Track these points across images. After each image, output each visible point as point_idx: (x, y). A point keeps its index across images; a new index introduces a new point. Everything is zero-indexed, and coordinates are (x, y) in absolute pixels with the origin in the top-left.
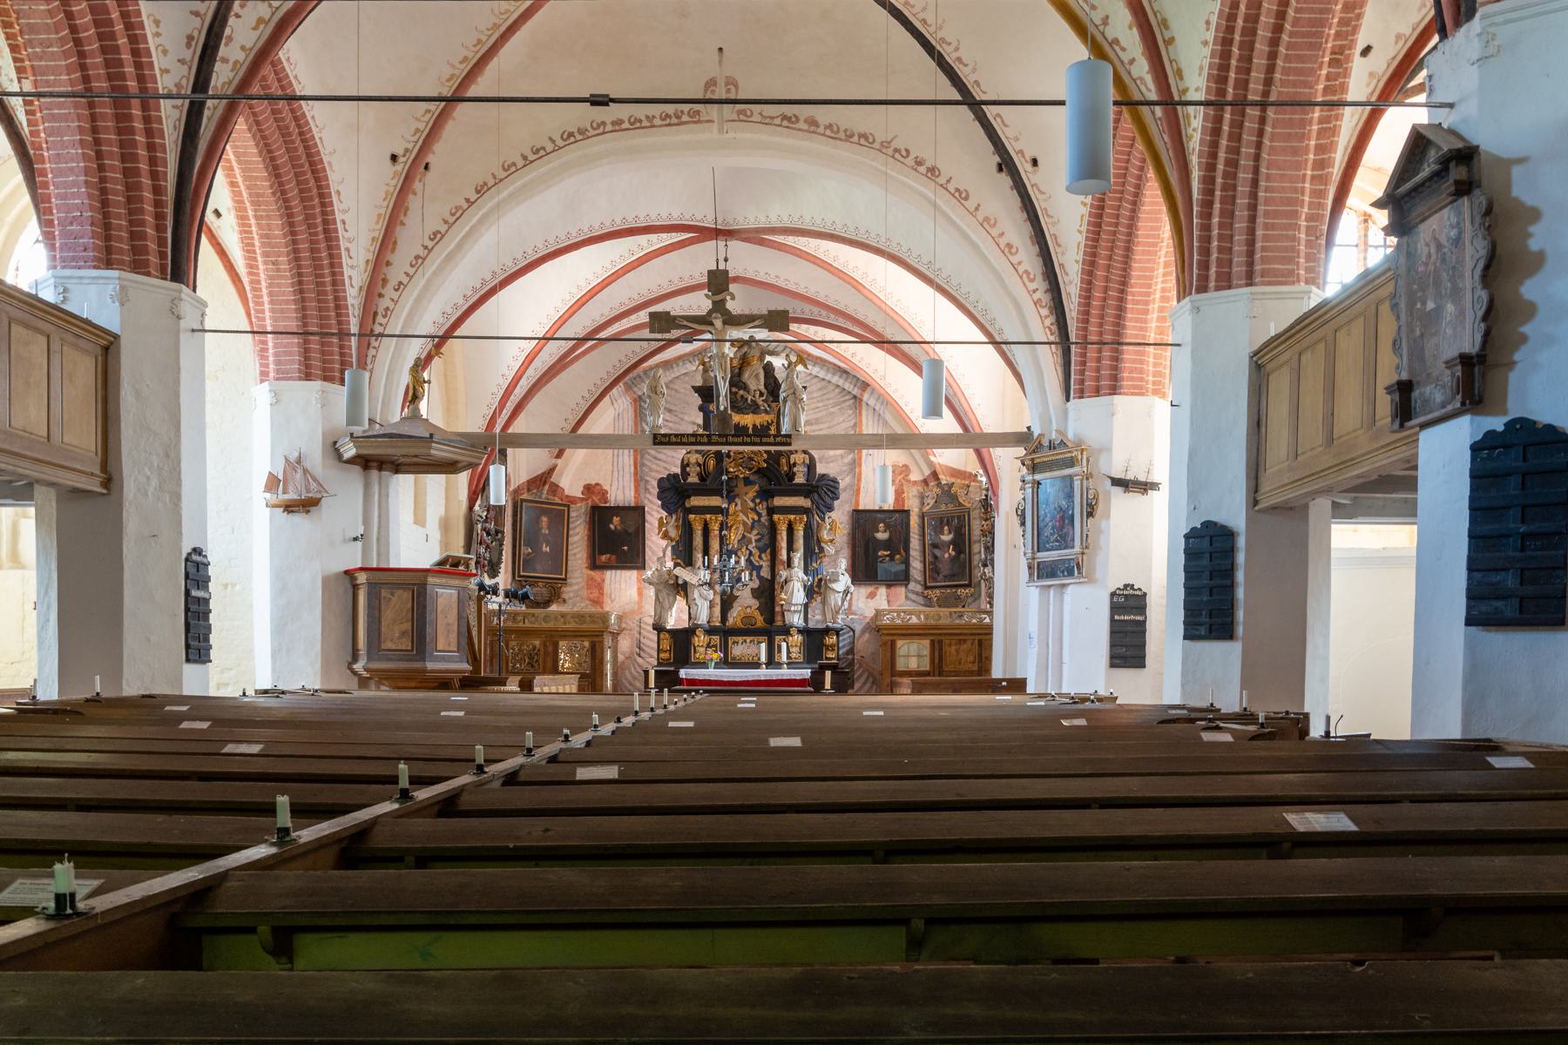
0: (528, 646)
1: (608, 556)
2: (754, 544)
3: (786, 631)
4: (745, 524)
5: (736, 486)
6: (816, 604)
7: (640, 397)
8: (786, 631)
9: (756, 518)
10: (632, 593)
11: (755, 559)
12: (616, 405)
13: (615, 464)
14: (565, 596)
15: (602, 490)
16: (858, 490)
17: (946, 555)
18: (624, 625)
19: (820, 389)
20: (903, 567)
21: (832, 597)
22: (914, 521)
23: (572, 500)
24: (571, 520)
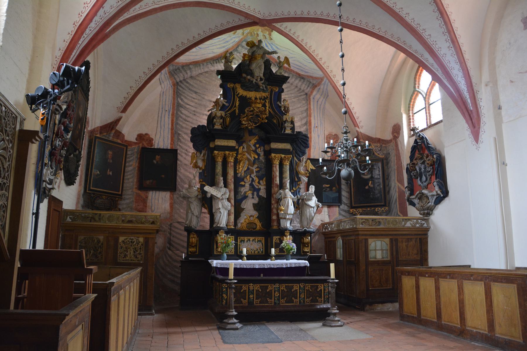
1: (151, 181)
2: (255, 174)
4: (248, 160)
7: (177, 83)
8: (282, 232)
9: (257, 157)
10: (166, 206)
11: (256, 184)
12: (163, 85)
13: (159, 122)
14: (120, 207)
15: (150, 138)
20: (337, 195)
23: (130, 143)
24: (128, 156)
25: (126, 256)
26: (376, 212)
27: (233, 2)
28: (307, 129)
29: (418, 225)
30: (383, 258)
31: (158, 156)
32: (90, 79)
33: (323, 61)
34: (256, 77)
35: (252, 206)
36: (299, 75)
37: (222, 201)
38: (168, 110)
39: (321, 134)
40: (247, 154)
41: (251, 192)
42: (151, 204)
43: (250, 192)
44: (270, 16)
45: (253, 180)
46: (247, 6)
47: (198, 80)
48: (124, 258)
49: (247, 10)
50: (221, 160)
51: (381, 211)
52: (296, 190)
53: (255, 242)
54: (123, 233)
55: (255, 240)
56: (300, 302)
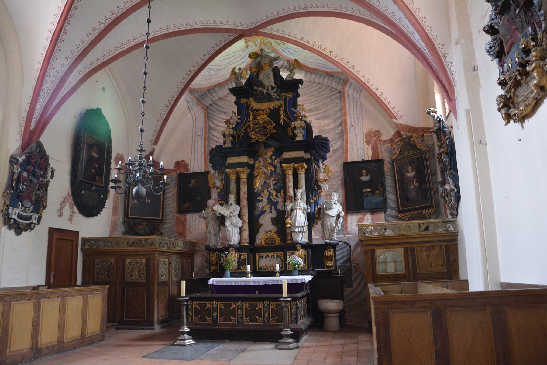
0: (107, 263)
1: (188, 204)
2: (272, 187)
3: (293, 247)
4: (265, 174)
5: (260, 149)
6: (317, 227)
7: (208, 107)
8: (293, 247)
9: (273, 169)
11: (273, 197)
12: (192, 112)
16: (347, 150)
17: (412, 187)
18: (197, 248)
19: (317, 90)
21: (328, 221)
22: (387, 167)
25: (132, 276)
26: (423, 214)
27: (207, 22)
28: (343, 129)
29: (440, 230)
30: (396, 271)
31: (193, 180)
32: (108, 123)
33: (334, 54)
34: (266, 88)
35: (270, 220)
36: (327, 73)
37: (231, 219)
38: (200, 135)
39: (359, 133)
40: (263, 168)
41: (269, 206)
42: (189, 226)
43: (267, 206)
44: (253, 24)
45: (270, 194)
46: (224, 22)
47: (227, 100)
48: (130, 277)
49: (226, 25)
50: (234, 178)
51: (428, 214)
52: (317, 200)
53: (274, 258)
54: (129, 256)
55: (274, 255)
56: (265, 322)
